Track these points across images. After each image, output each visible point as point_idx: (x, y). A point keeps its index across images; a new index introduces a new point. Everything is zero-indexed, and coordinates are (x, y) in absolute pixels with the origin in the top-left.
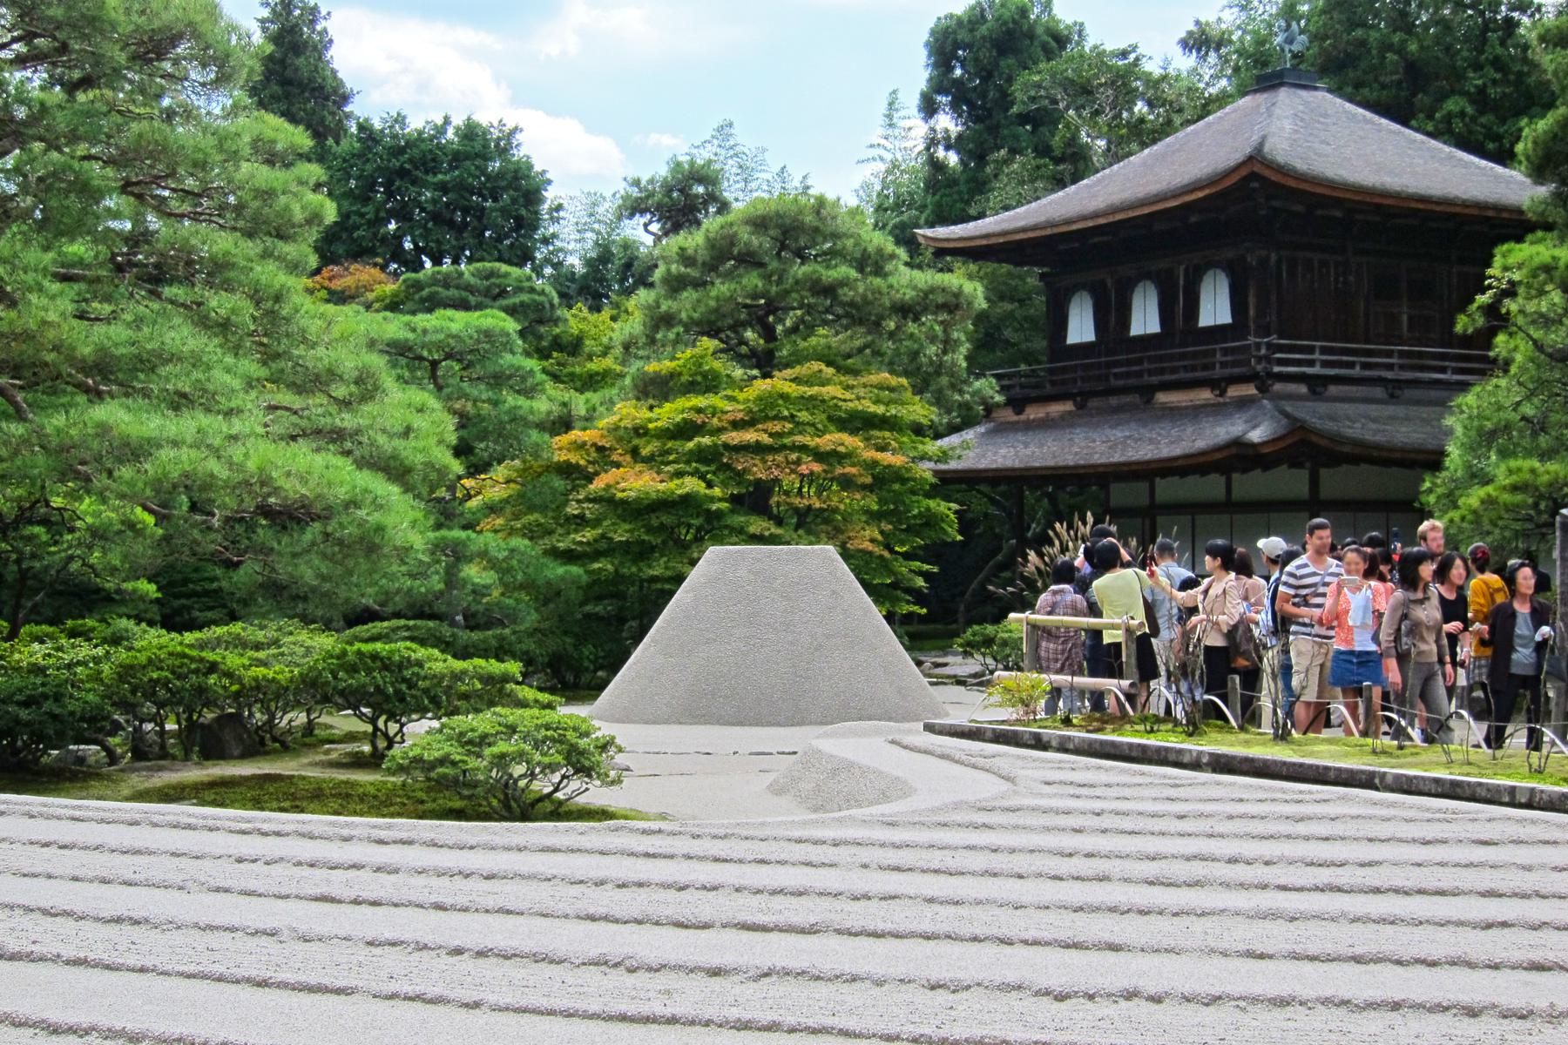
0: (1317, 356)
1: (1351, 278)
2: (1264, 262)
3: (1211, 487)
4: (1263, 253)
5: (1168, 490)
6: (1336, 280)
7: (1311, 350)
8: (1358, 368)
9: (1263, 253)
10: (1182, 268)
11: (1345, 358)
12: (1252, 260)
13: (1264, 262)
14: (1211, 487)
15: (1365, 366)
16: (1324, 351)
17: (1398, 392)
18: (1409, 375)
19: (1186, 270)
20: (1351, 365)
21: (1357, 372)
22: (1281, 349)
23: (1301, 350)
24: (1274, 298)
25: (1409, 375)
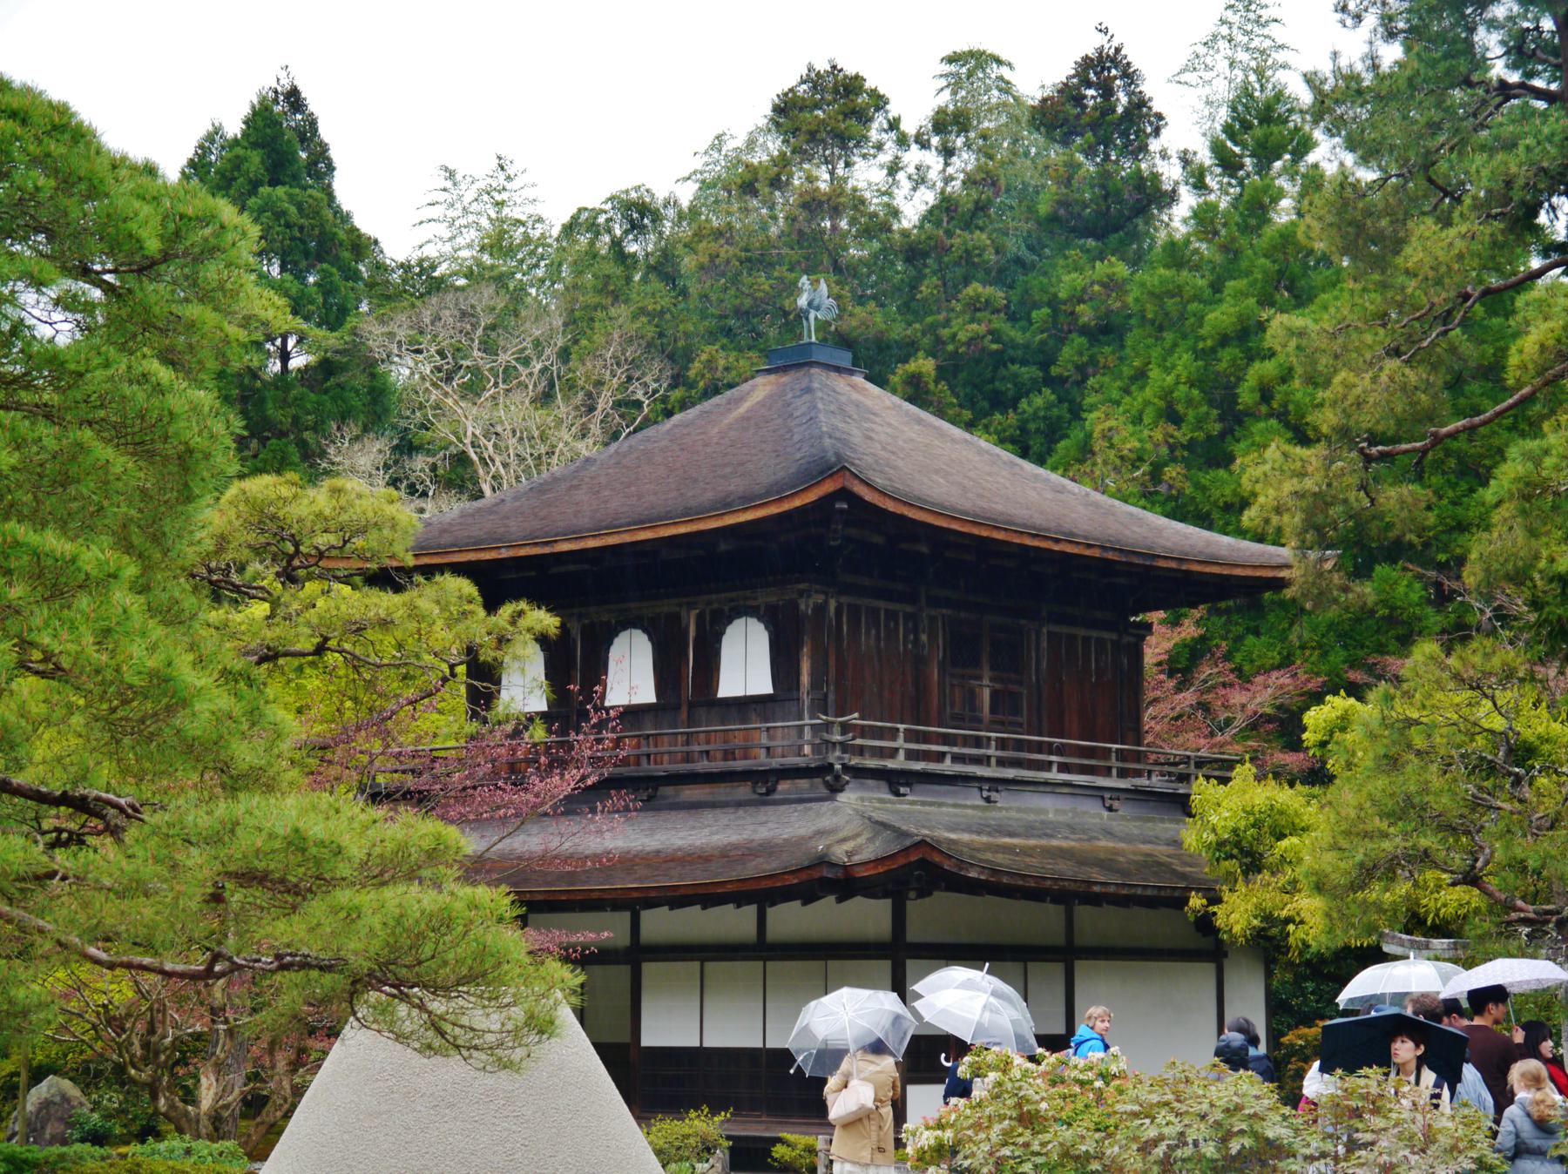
0: (900, 742)
1: (924, 637)
2: (821, 609)
3: (736, 922)
4: (820, 599)
5: (659, 924)
6: (905, 637)
7: (893, 734)
8: (948, 761)
9: (820, 599)
10: (694, 613)
11: (934, 748)
12: (806, 606)
13: (821, 609)
14: (736, 922)
15: (957, 758)
16: (911, 736)
17: (994, 795)
18: (1010, 773)
19: (700, 618)
20: (940, 757)
21: (947, 767)
22: (864, 732)
23: (880, 733)
24: (832, 662)
25: (1010, 773)
